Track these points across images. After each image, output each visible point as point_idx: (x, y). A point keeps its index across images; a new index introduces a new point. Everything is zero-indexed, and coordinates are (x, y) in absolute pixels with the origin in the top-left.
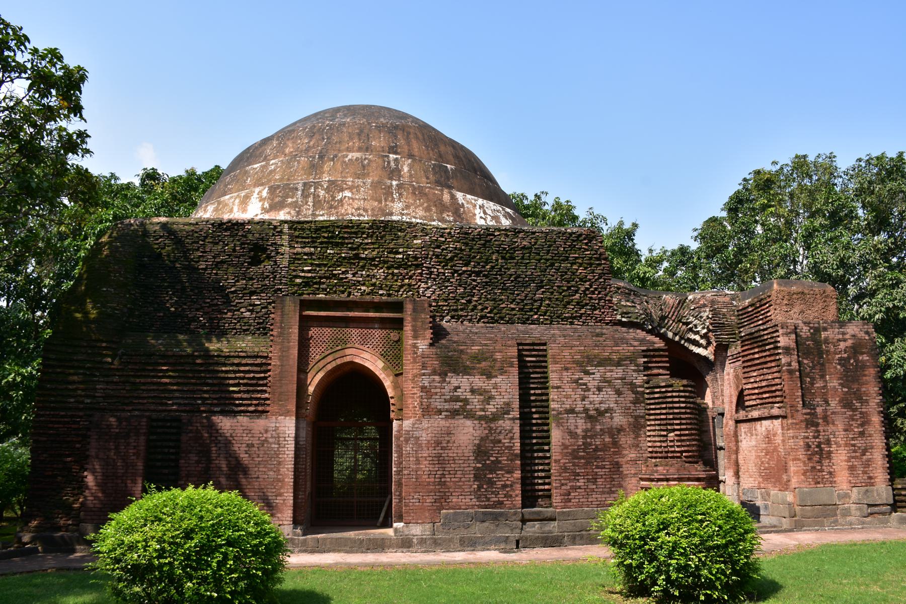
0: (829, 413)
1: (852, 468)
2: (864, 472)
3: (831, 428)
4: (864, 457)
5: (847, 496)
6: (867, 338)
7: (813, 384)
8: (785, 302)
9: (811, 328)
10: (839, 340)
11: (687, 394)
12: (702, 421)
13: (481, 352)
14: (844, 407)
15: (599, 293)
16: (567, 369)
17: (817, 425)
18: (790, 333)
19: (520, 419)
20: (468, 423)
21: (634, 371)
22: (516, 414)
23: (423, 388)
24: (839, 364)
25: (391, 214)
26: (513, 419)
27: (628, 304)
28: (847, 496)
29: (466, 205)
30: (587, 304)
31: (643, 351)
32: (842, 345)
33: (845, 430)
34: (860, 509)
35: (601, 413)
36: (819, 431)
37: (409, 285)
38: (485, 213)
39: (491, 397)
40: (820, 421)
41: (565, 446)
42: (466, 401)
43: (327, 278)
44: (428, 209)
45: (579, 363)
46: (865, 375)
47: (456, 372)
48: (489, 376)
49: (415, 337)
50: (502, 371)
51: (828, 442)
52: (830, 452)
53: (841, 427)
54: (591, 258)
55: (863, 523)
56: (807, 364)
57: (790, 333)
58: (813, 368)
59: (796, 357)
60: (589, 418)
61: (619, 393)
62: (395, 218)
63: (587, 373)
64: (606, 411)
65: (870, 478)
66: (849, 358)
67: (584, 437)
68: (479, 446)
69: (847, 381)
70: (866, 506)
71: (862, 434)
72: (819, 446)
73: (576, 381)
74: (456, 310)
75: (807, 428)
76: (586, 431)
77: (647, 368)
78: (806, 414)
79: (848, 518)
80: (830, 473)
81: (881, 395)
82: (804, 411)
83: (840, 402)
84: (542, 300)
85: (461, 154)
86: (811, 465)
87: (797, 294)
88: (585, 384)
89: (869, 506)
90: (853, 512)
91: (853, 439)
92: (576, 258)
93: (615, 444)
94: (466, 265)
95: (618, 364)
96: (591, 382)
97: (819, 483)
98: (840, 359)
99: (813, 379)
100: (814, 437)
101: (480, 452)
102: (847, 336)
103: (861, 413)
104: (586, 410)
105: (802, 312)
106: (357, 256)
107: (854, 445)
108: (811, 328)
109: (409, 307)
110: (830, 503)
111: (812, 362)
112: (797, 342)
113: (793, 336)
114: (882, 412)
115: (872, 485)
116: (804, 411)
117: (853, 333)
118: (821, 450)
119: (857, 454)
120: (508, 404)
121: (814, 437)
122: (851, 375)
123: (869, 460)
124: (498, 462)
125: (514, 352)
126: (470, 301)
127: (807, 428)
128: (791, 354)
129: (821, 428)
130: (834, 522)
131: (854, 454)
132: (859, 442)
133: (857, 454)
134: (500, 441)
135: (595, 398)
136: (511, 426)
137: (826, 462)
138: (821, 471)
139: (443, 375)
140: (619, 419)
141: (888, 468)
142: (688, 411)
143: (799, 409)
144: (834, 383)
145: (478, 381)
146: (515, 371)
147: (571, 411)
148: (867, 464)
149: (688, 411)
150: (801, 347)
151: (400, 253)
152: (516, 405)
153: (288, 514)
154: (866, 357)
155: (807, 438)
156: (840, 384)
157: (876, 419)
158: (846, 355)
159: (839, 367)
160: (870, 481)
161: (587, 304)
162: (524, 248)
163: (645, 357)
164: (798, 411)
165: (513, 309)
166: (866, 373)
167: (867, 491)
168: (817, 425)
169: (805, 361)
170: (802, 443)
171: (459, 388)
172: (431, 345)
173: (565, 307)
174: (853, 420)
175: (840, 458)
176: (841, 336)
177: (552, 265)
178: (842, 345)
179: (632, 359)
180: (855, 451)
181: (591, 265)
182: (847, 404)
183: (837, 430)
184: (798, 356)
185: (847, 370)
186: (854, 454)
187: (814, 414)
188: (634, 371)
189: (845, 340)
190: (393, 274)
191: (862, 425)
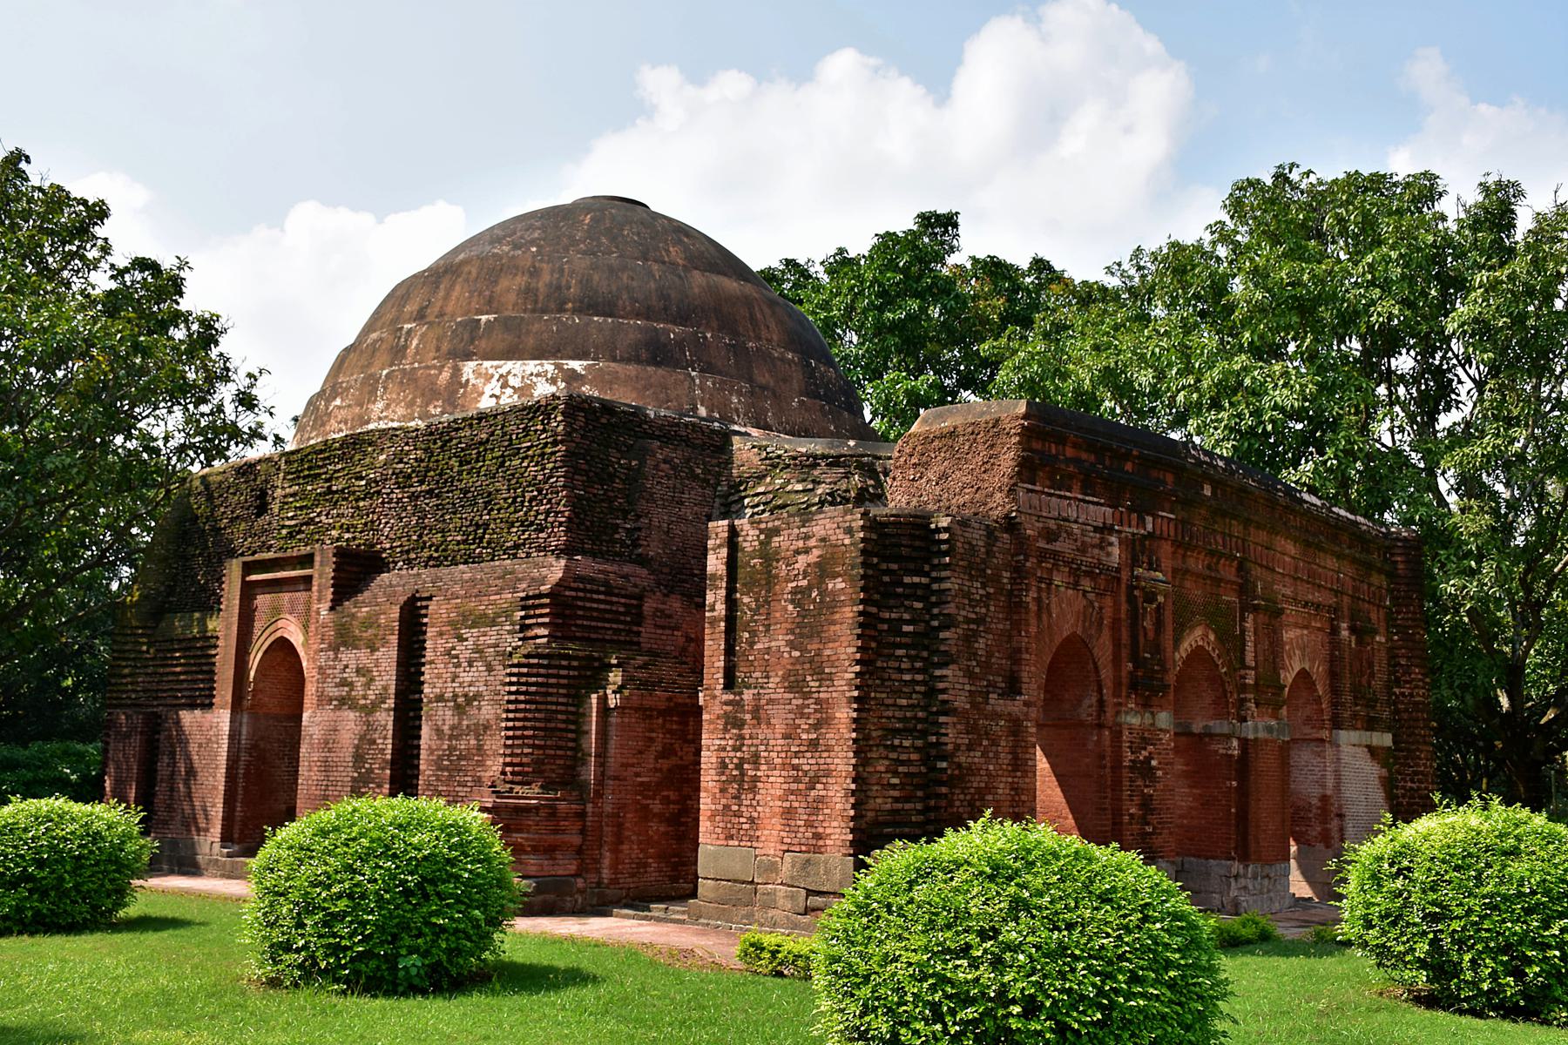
0: (763, 702)
1: (789, 813)
2: (809, 824)
3: (763, 732)
4: (813, 793)
5: (772, 868)
6: (847, 542)
7: (751, 644)
8: (914, 460)
9: (762, 531)
10: (797, 552)
11: (525, 670)
12: (584, 715)
13: (369, 615)
14: (789, 689)
15: (549, 501)
16: (441, 634)
17: (740, 724)
18: (719, 546)
19: (395, 710)
20: (352, 715)
21: (509, 632)
22: (391, 703)
23: (320, 668)
24: (792, 601)
25: (368, 422)
26: (388, 710)
27: (799, 487)
28: (772, 868)
29: (472, 381)
30: (532, 523)
31: (522, 599)
32: (802, 560)
33: (786, 737)
34: (792, 897)
35: (469, 700)
36: (742, 737)
37: (372, 522)
38: (505, 385)
39: (372, 680)
40: (748, 717)
41: (431, 751)
42: (351, 685)
43: (307, 524)
44: (410, 405)
45: (450, 623)
46: (834, 623)
47: (345, 644)
48: (373, 650)
49: (319, 600)
50: (385, 643)
51: (755, 760)
52: (756, 779)
53: (780, 729)
54: (546, 445)
55: (795, 926)
56: (747, 605)
57: (719, 546)
58: (756, 612)
59: (723, 592)
60: (458, 707)
61: (490, 669)
62: (371, 426)
63: (461, 639)
64: (475, 698)
65: (817, 836)
66: (810, 588)
67: (451, 738)
68: (357, 747)
69: (801, 635)
70: (803, 892)
71: (813, 745)
72: (739, 766)
73: (448, 653)
74: (408, 552)
75: (726, 730)
76: (453, 728)
77: (524, 628)
78: (726, 703)
79: (771, 913)
80: (752, 820)
81: (858, 662)
82: (725, 697)
83: (784, 678)
84: (486, 525)
85: (457, 301)
86: (724, 801)
87: (942, 437)
88: (457, 657)
89: (810, 893)
90: (781, 902)
91: (796, 755)
92: (529, 448)
93: (480, 748)
94: (421, 483)
95: (493, 623)
96: (464, 651)
97: (731, 837)
98: (795, 591)
99: (753, 633)
100: (736, 749)
101: (359, 758)
102: (812, 543)
103: (818, 701)
104: (455, 696)
105: (944, 476)
106: (329, 491)
107: (796, 768)
108: (762, 531)
109: (317, 558)
110: (743, 877)
111: (757, 600)
112: (732, 564)
113: (724, 552)
114: (856, 700)
115: (817, 850)
116: (725, 697)
117: (823, 532)
118: (743, 774)
119: (802, 786)
120: (385, 688)
121: (736, 749)
122: (809, 627)
123: (820, 800)
124: (371, 770)
125: (395, 613)
126: (420, 536)
127: (726, 730)
128: (717, 588)
129: (746, 732)
130: (747, 916)
131: (794, 786)
132: (807, 763)
133: (802, 786)
134: (374, 742)
135: (466, 677)
136: (385, 719)
137: (746, 799)
138: (738, 814)
139: (336, 650)
140: (487, 711)
141: (852, 819)
142: (522, 698)
143: (717, 693)
144: (780, 641)
145: (362, 656)
146: (394, 639)
147: (440, 698)
148: (816, 806)
149: (522, 698)
150: (741, 573)
151: (362, 478)
152: (392, 690)
153: (216, 830)
154: (840, 584)
155: (724, 749)
156: (790, 644)
157: (844, 714)
158: (805, 583)
159: (790, 607)
160: (816, 844)
161: (532, 523)
162: (481, 443)
163: (523, 608)
164: (715, 697)
165: (458, 543)
166: (837, 616)
167: (808, 861)
168: (740, 724)
169: (746, 600)
170: (714, 760)
171: (346, 666)
172: (332, 609)
173: (509, 533)
174: (802, 715)
175: (773, 786)
176: (801, 544)
177: (502, 465)
178: (802, 560)
179: (508, 614)
180: (797, 780)
181: (543, 455)
182: (795, 685)
183: (771, 739)
184: (731, 590)
185: (803, 613)
186: (794, 786)
187: (738, 704)
188: (509, 632)
189: (807, 551)
190: (358, 508)
191: (816, 727)
